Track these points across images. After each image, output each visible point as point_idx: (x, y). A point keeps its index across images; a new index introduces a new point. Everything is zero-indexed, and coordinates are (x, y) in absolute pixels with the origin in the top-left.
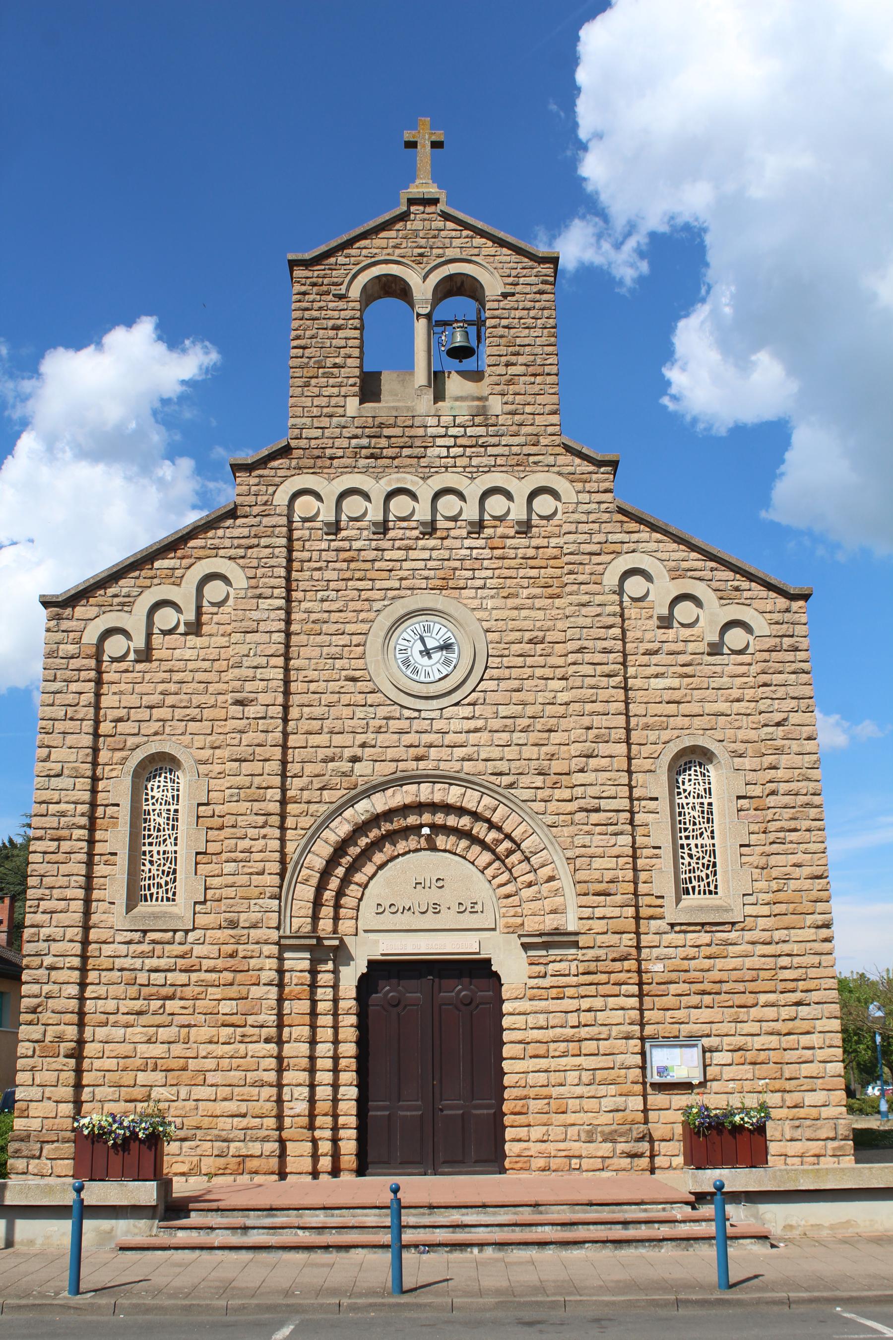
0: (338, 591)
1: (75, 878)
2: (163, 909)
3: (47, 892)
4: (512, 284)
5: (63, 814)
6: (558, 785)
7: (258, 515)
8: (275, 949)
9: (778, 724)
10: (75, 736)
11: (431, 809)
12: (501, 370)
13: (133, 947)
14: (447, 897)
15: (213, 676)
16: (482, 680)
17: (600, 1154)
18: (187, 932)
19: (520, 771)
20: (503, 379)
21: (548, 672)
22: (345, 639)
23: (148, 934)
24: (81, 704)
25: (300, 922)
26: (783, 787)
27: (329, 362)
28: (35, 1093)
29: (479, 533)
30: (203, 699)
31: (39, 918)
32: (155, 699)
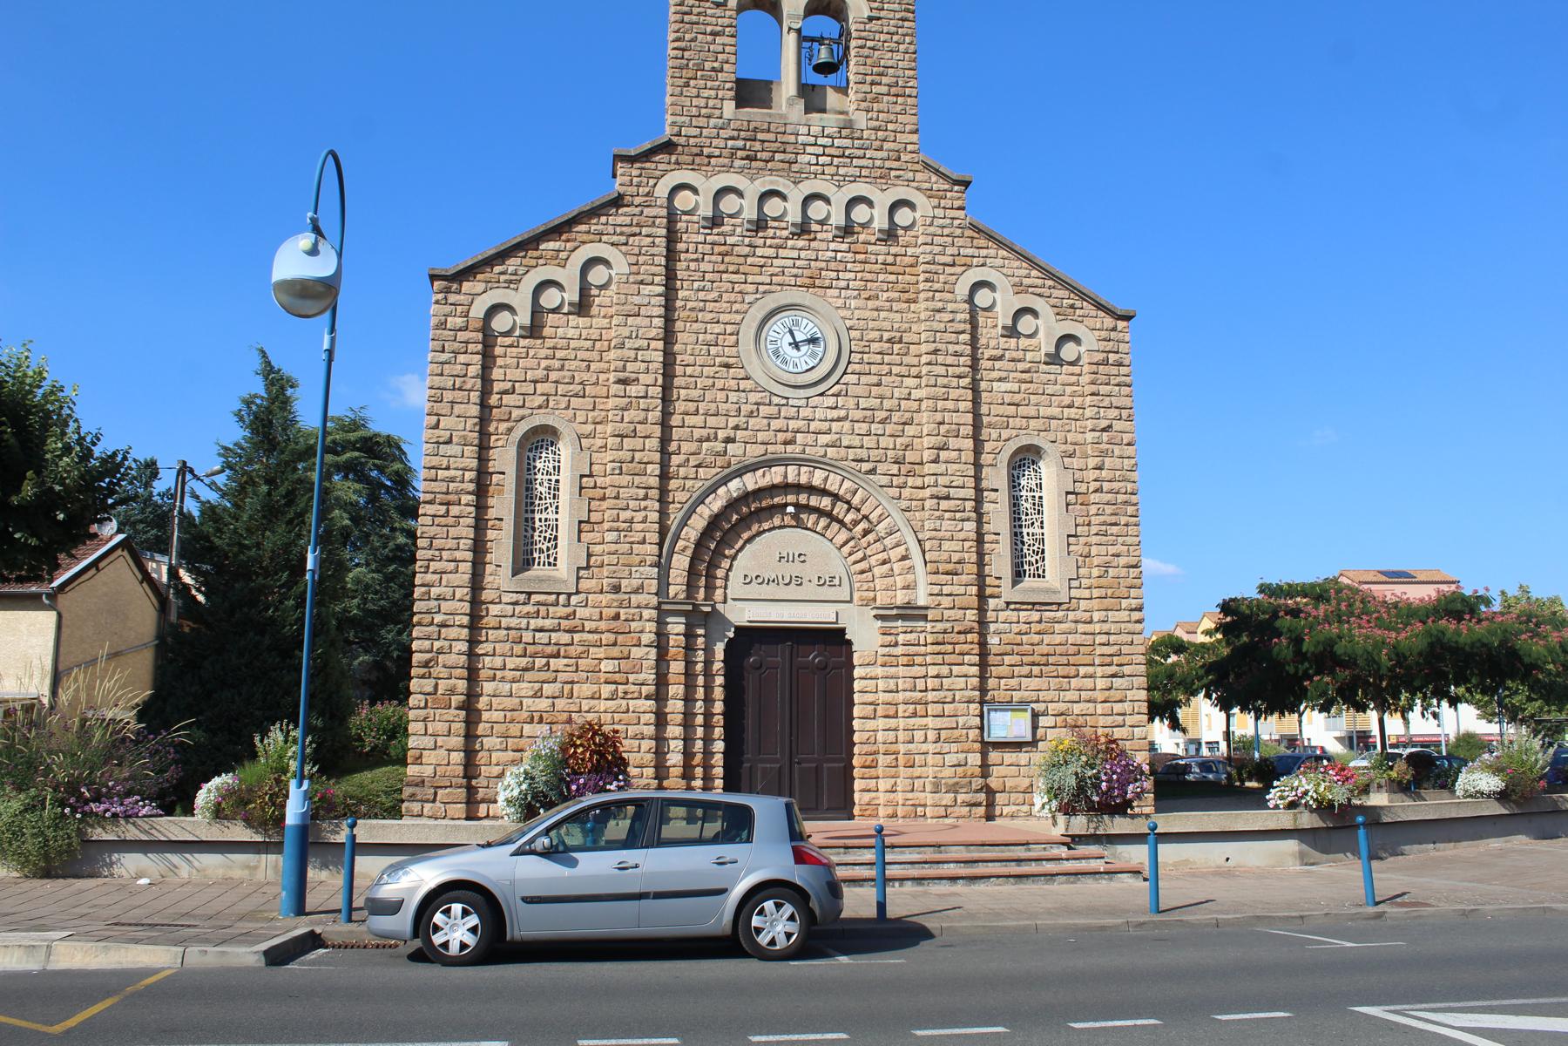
0: (713, 282)
1: (462, 541)
2: (547, 573)
3: (437, 553)
4: (877, 9)
5: (452, 480)
6: (912, 474)
7: (639, 205)
8: (654, 613)
9: (1104, 430)
10: (463, 406)
11: (795, 490)
12: (866, 88)
13: (518, 608)
14: (808, 571)
15: (595, 355)
16: (845, 373)
17: (944, 803)
18: (569, 595)
19: (878, 459)
20: (869, 96)
21: (904, 370)
22: (718, 328)
23: (533, 596)
24: (469, 375)
25: (677, 589)
26: (1106, 486)
27: (708, 65)
28: (428, 742)
29: (843, 238)
30: (585, 376)
31: (430, 577)
32: (540, 374)
